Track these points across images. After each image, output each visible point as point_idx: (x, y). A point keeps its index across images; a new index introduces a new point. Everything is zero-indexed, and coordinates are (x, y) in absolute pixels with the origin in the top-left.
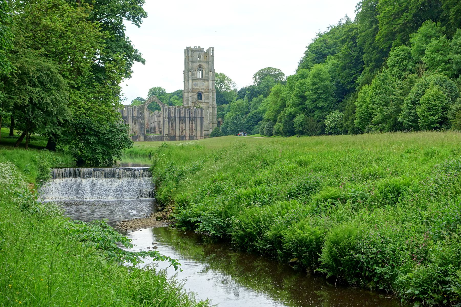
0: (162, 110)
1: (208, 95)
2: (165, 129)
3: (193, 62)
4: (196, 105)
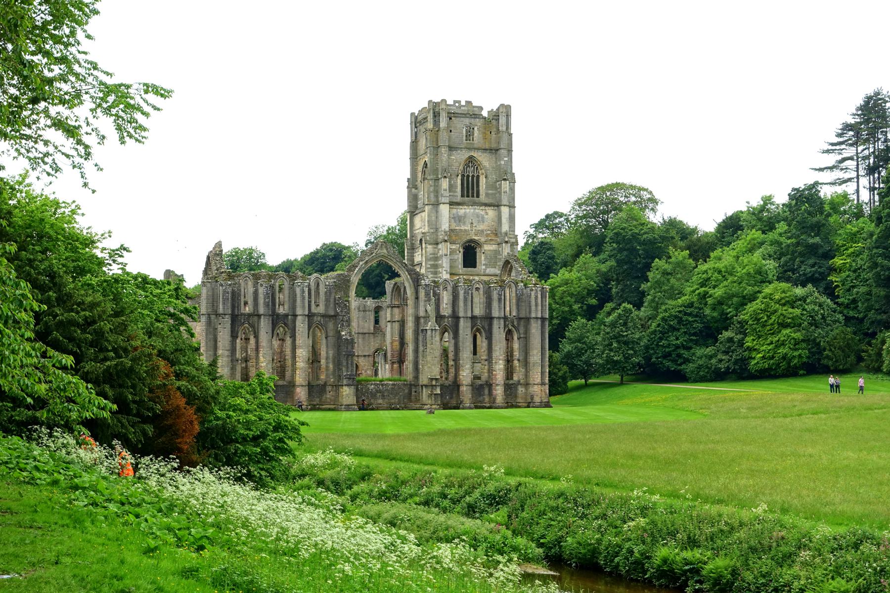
0: (410, 292)
1: (497, 253)
3: (451, 148)
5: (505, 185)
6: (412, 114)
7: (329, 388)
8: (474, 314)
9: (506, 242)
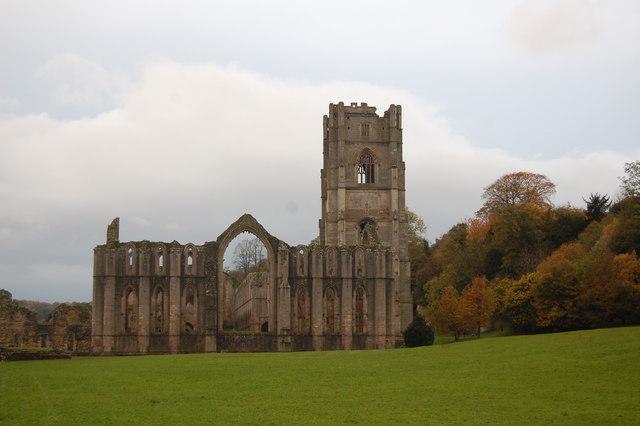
2: (280, 313)
5: (394, 172)
6: (325, 117)
7: (200, 338)
8: (328, 274)
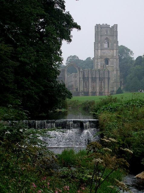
0: (78, 72)
1: (113, 61)
4: (105, 68)
5: (115, 44)
9: (115, 58)
